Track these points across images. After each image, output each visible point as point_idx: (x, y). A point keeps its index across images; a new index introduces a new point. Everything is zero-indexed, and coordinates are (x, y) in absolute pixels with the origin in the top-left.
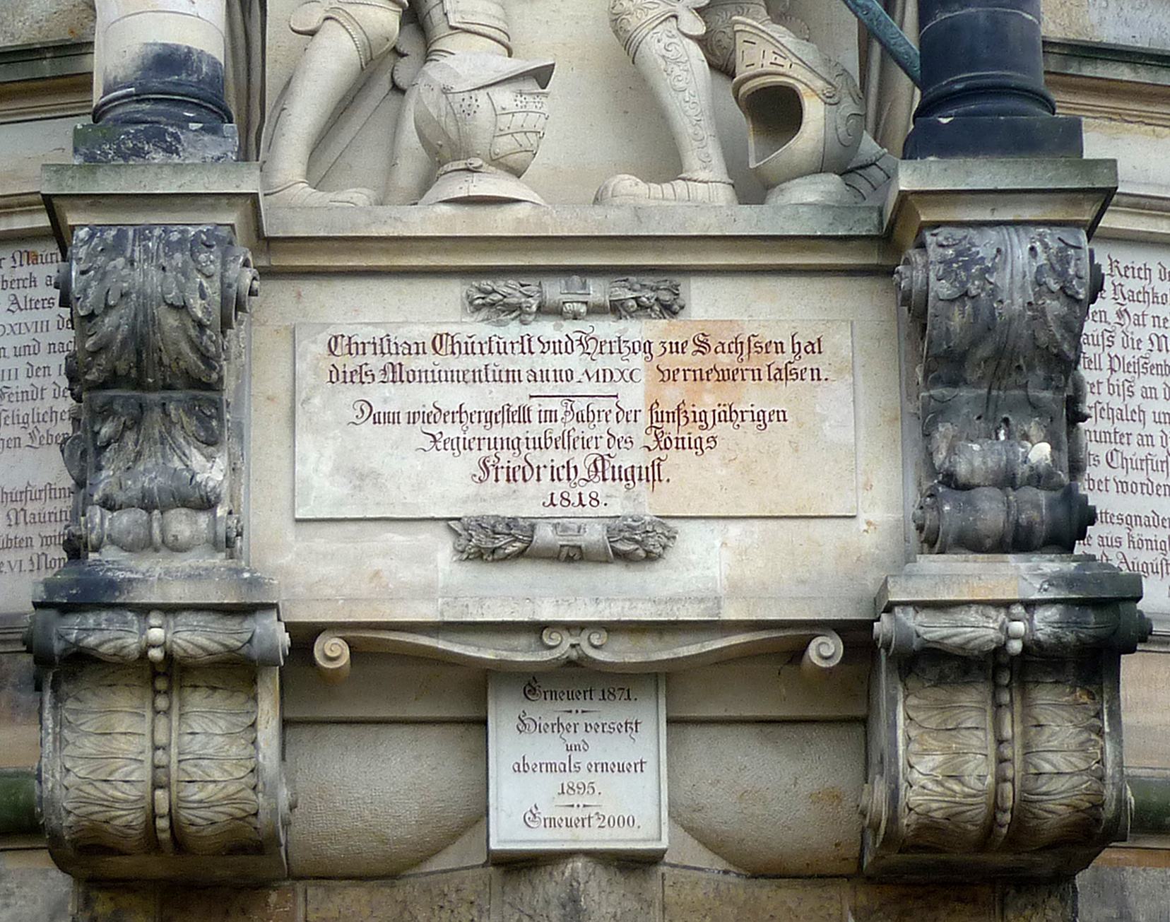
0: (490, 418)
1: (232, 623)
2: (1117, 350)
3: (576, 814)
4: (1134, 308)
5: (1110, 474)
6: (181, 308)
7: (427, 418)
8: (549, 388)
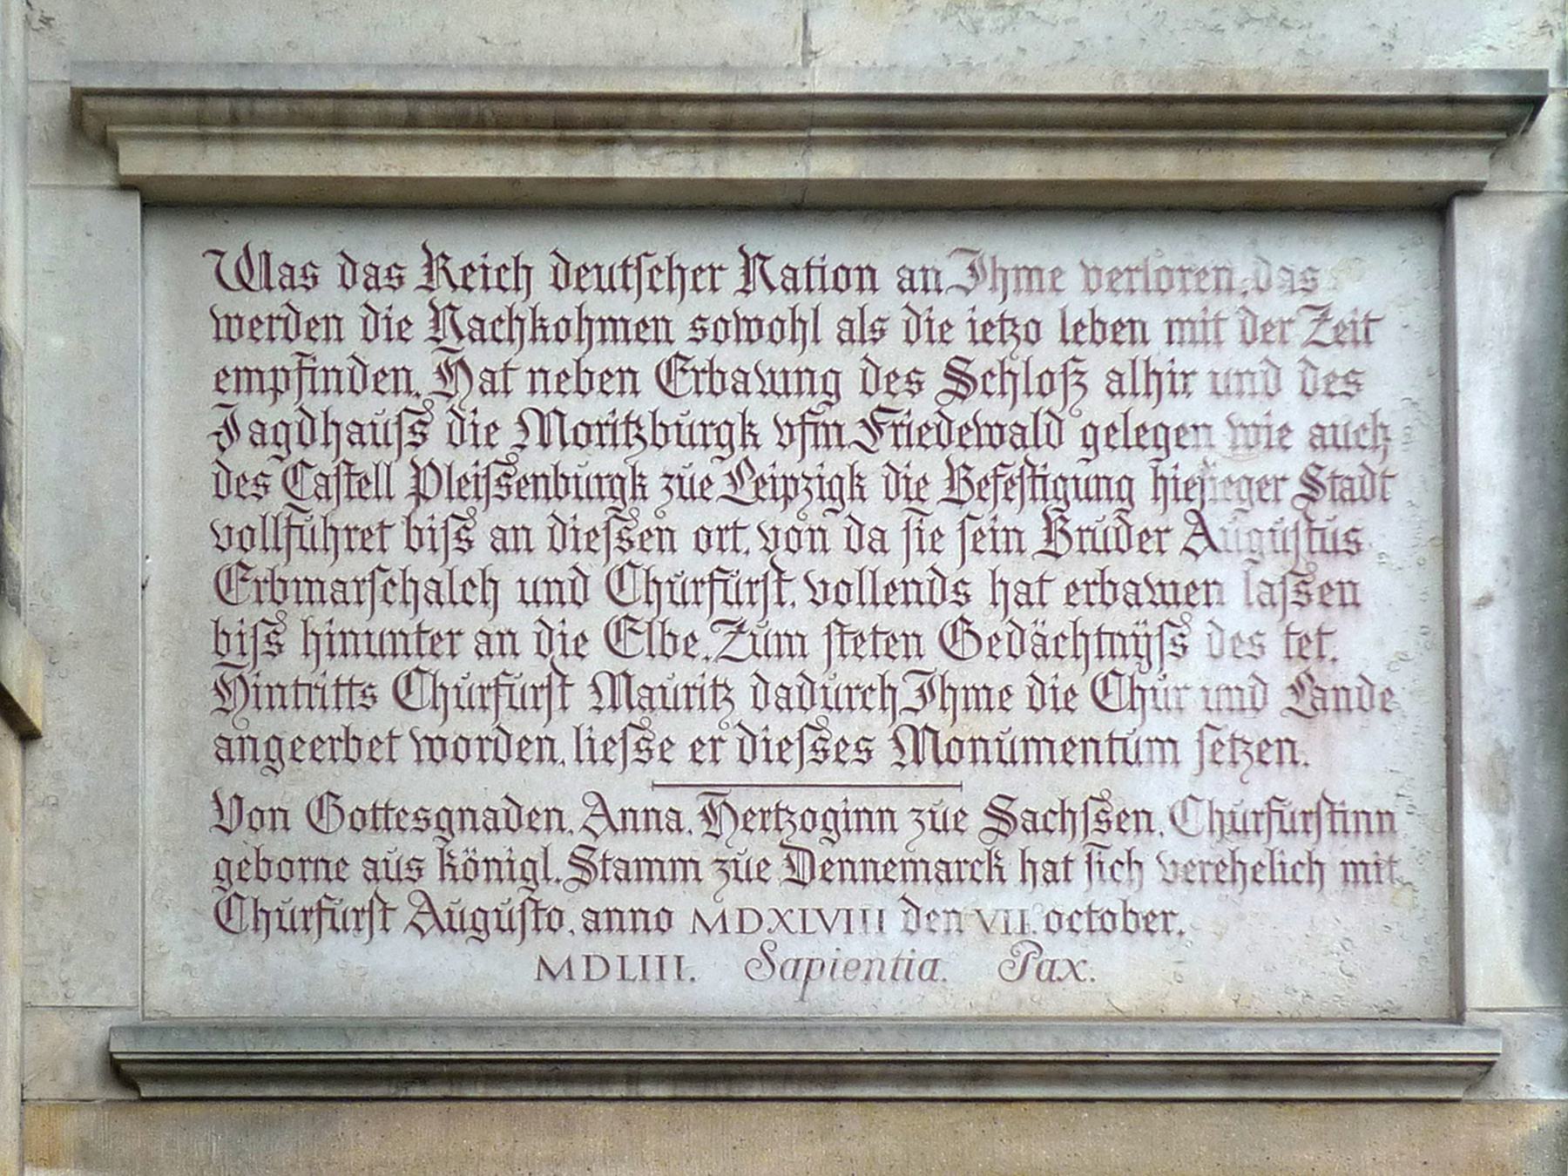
2: (435, 450)
4: (480, 357)
5: (401, 722)
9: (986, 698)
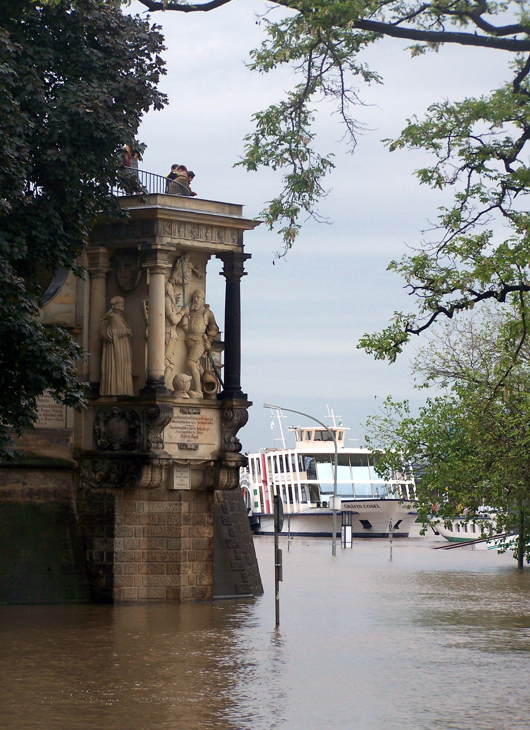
0: (182, 428)
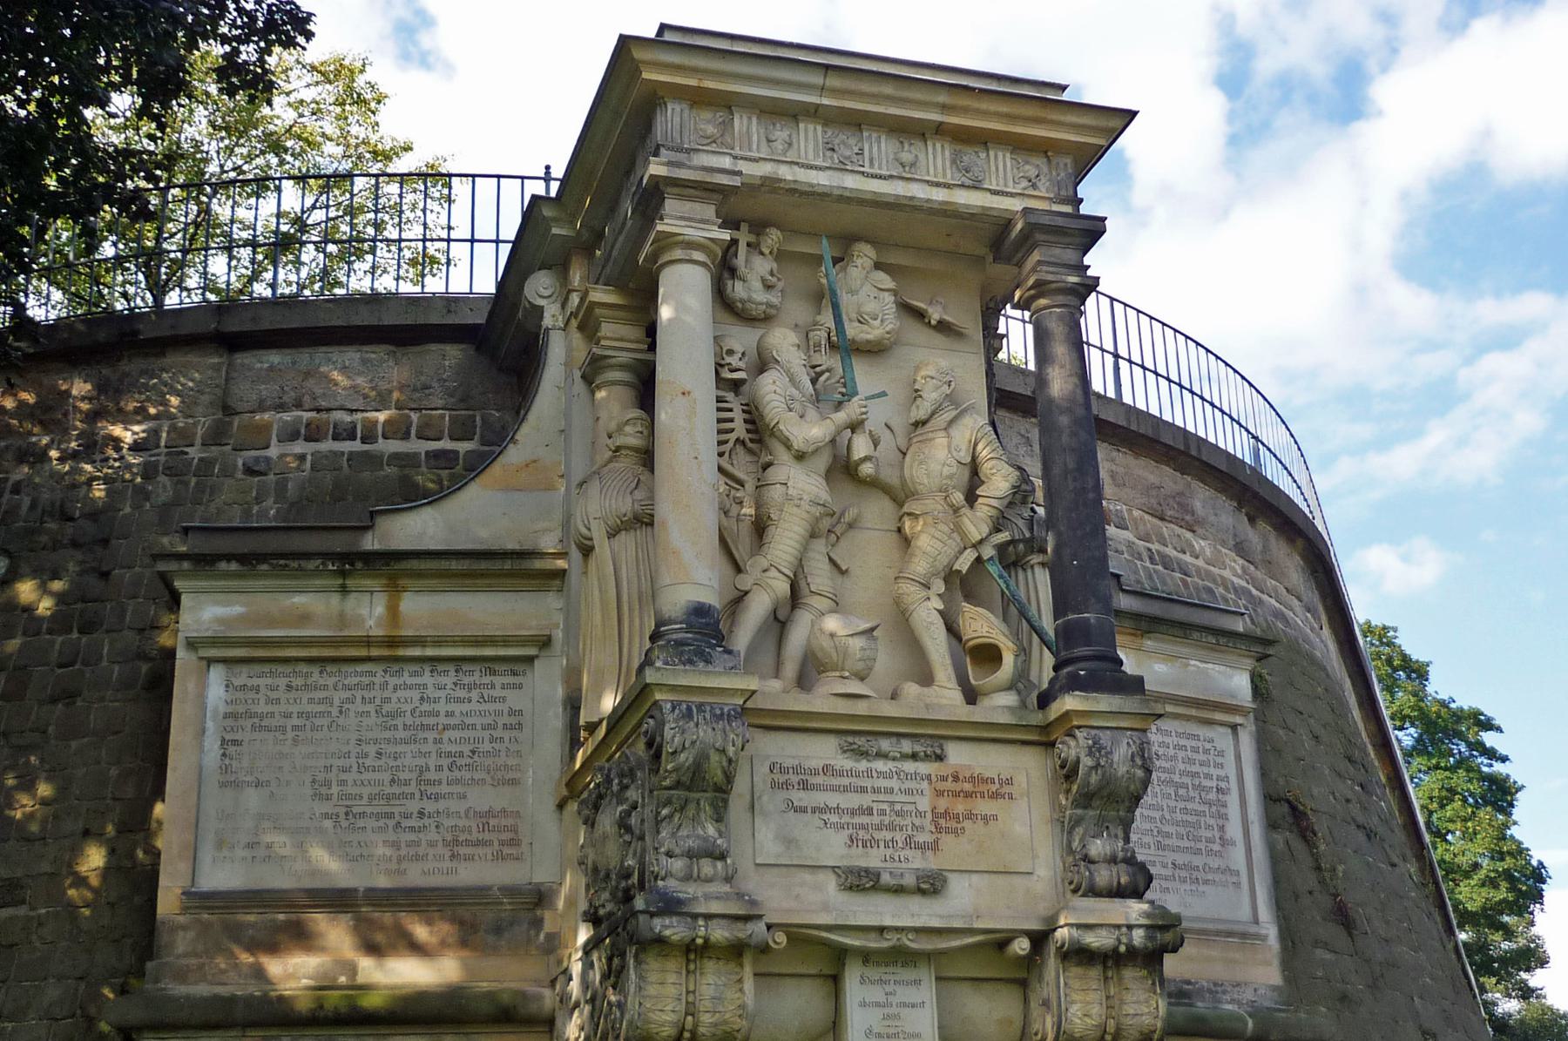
0: (853, 813)
1: (740, 925)
3: (892, 1031)
6: (723, 751)
7: (821, 811)
8: (881, 797)
9: (1168, 835)
